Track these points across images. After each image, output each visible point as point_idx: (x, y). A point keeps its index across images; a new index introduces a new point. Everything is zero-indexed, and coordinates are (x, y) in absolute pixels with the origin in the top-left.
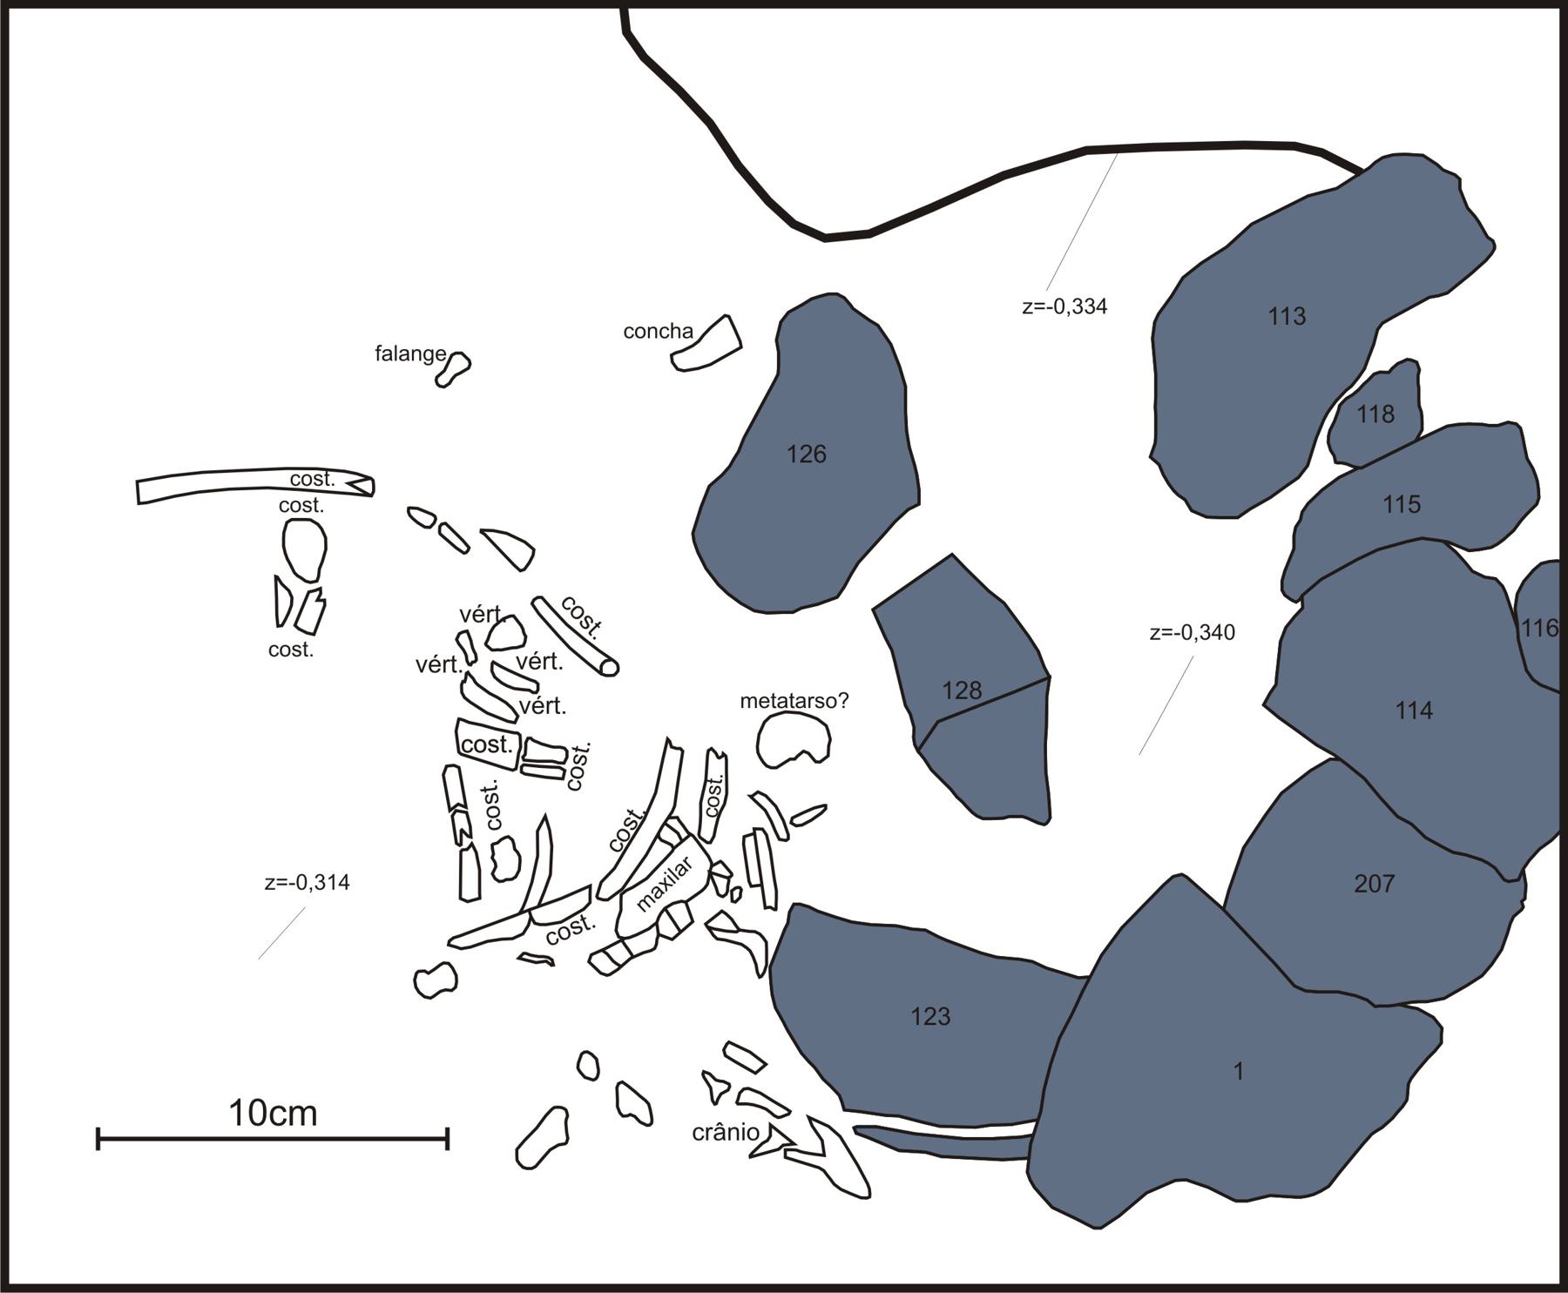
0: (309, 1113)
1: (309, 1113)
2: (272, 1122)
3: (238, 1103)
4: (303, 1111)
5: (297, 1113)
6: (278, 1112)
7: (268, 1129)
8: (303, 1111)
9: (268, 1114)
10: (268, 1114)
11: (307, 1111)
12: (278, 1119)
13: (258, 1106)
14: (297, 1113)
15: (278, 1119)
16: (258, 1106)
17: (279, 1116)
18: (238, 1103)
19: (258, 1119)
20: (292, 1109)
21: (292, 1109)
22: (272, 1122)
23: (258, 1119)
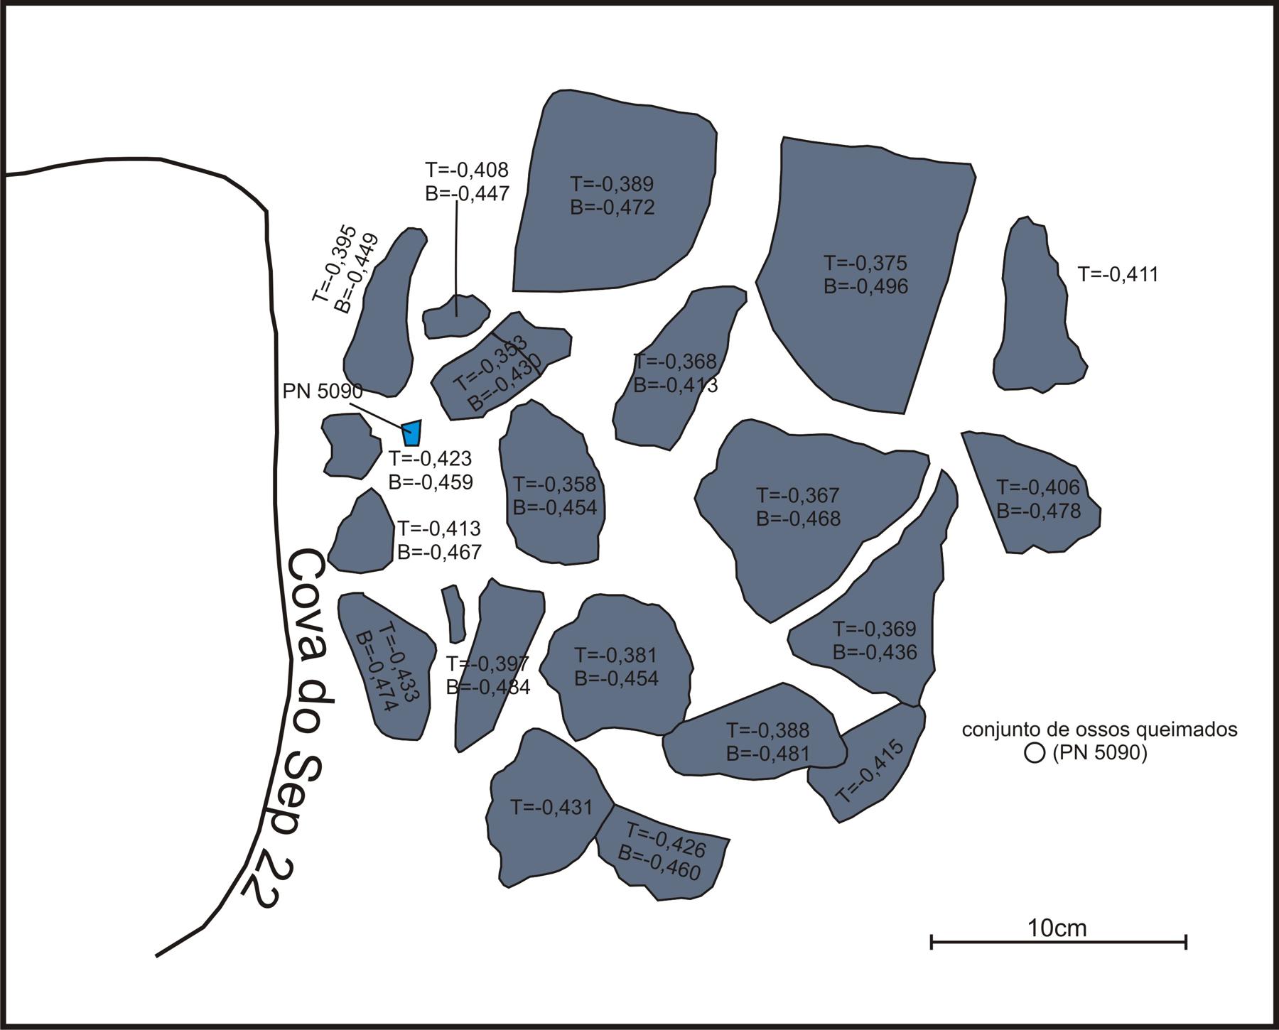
0: (1081, 928)
1: (1081, 928)
2: (1053, 933)
3: (1034, 921)
5: (1073, 928)
7: (1054, 937)
12: (1061, 932)
13: (1047, 923)
14: (1073, 928)
15: (1061, 932)
16: (1047, 923)
17: (1061, 930)
18: (1034, 921)
19: (1047, 931)
22: (1053, 933)
23: (1047, 931)
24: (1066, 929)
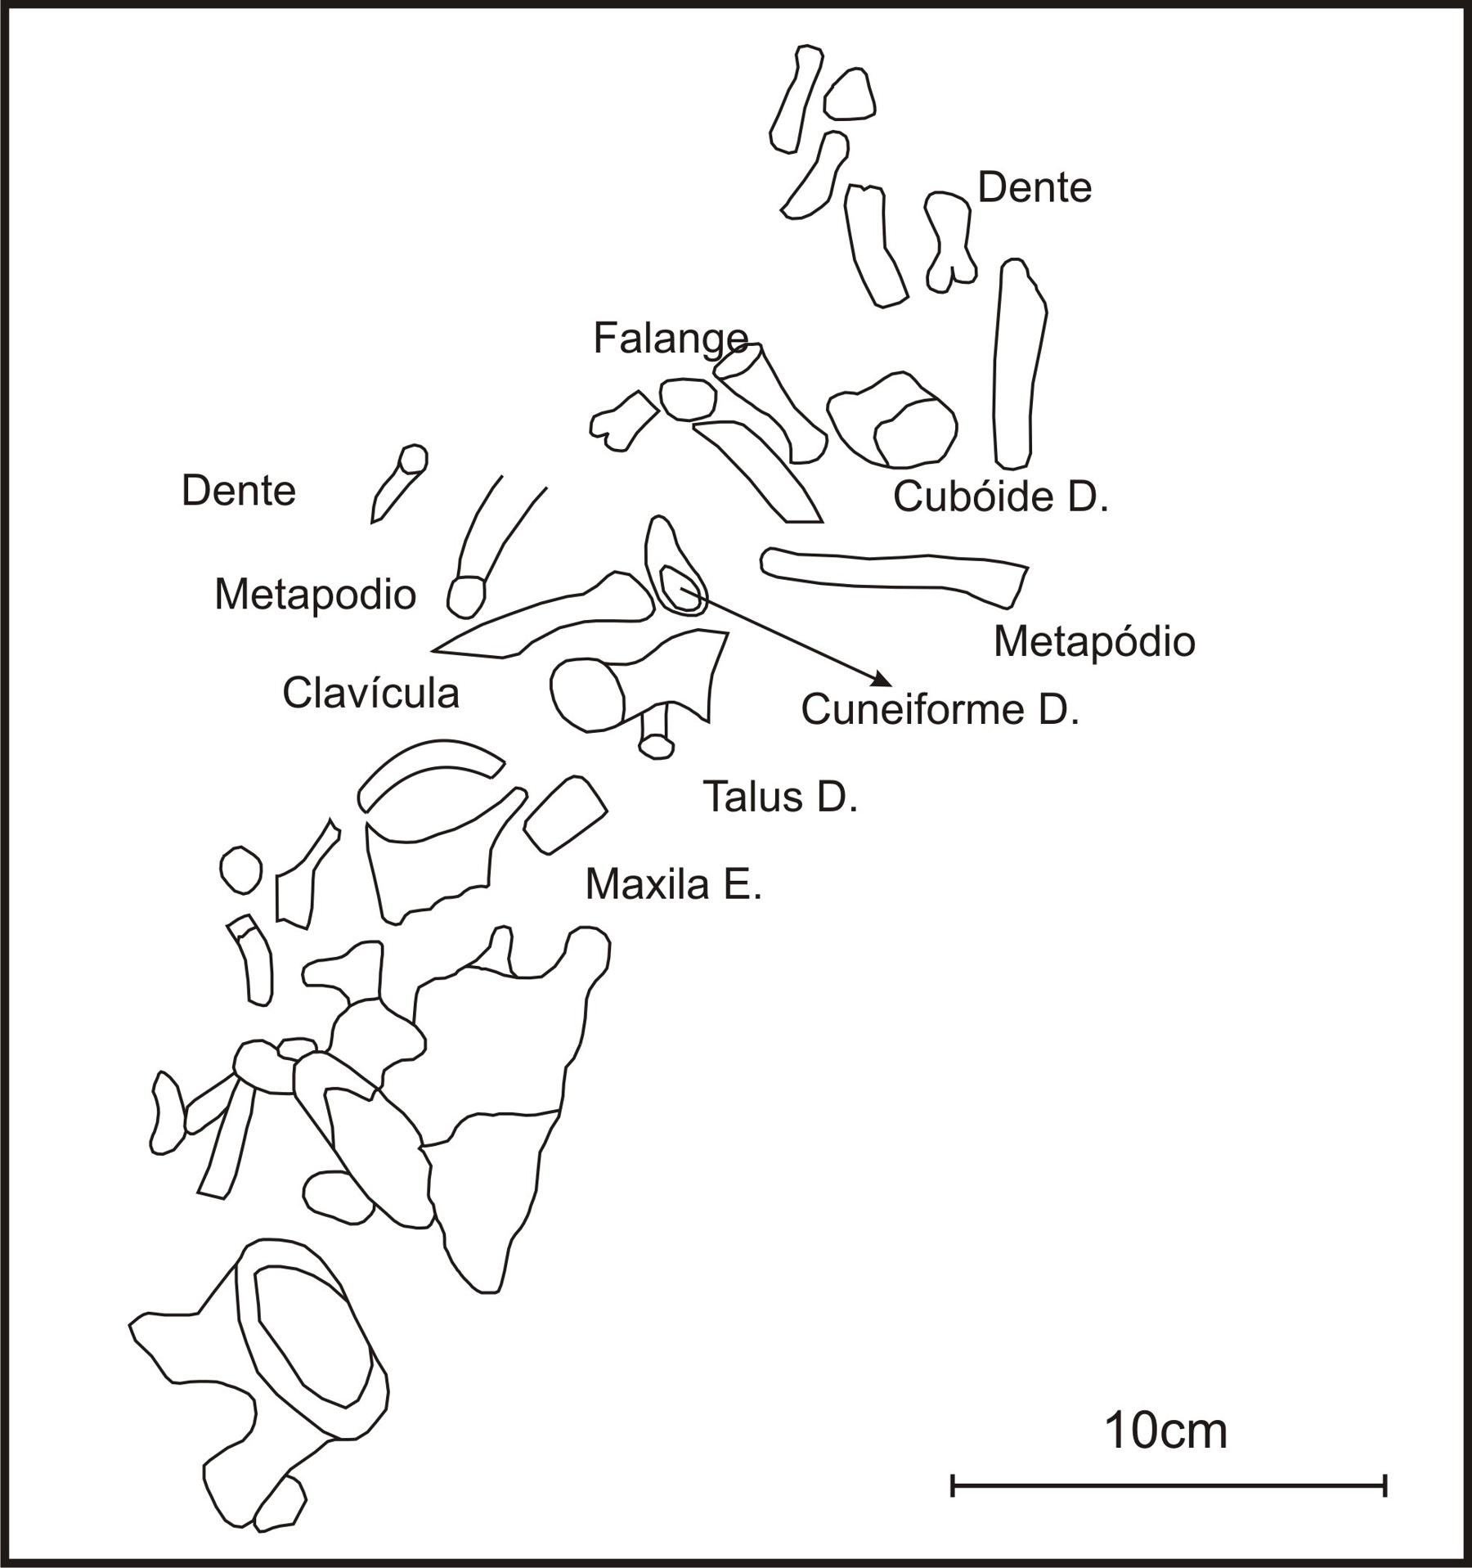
0: (1216, 1431)
1: (1216, 1431)
4: (1208, 1427)
5: (1200, 1430)
6: (1173, 1428)
9: (1160, 1433)
10: (1160, 1433)
11: (1212, 1430)
12: (1173, 1440)
13: (1145, 1423)
14: (1200, 1430)
15: (1173, 1440)
16: (1145, 1423)
17: (1174, 1435)
19: (1145, 1438)
20: (1192, 1425)
21: (1192, 1425)
23: (1145, 1435)
24: (1185, 1433)
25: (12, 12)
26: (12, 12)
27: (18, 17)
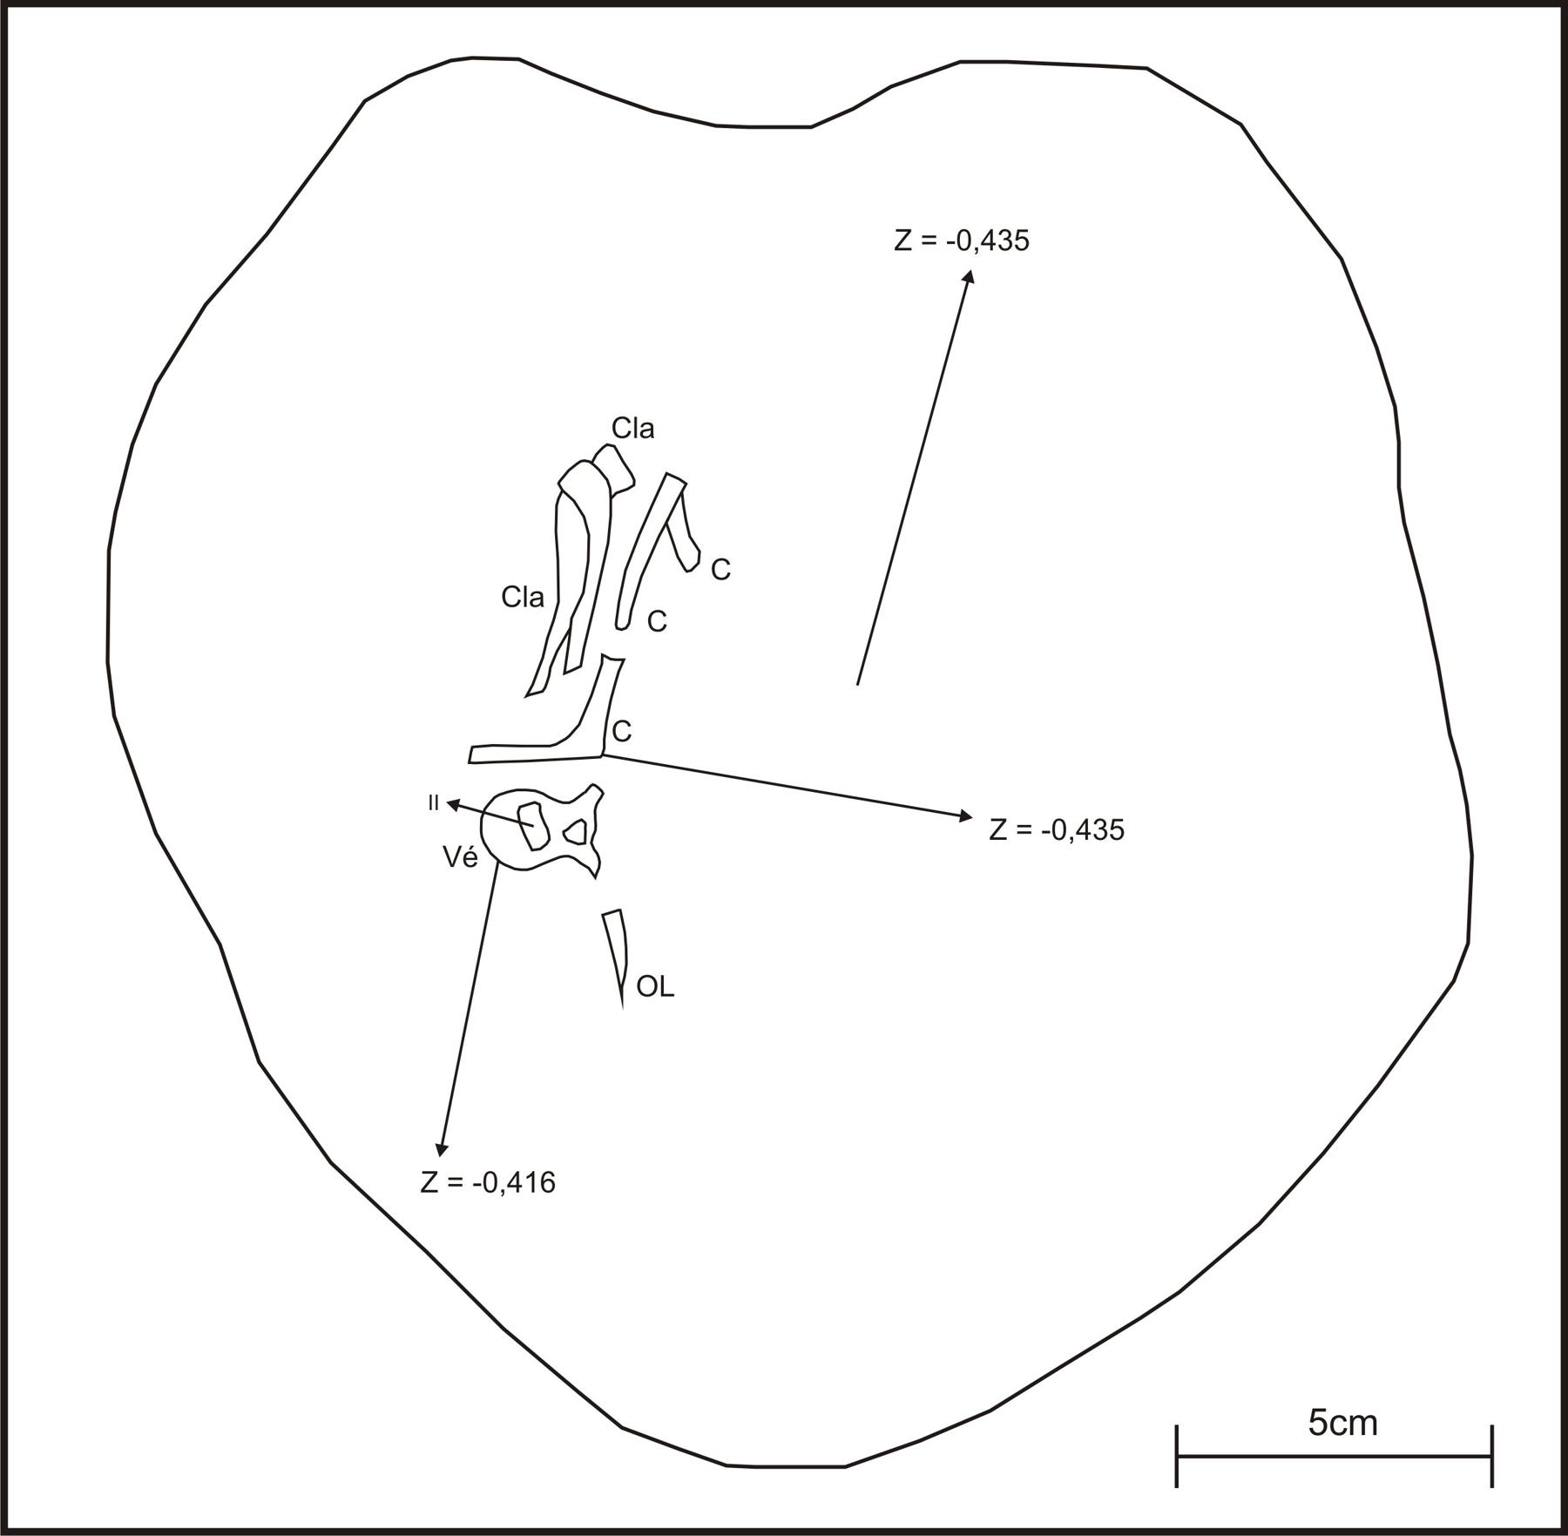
0: (1369, 1422)
1: (1369, 1422)
4: (1363, 1420)
5: (1358, 1422)
6: (1338, 1422)
8: (1363, 1420)
10: (1329, 1426)
11: (1366, 1422)
12: (1338, 1429)
14: (1358, 1422)
15: (1338, 1429)
20: (1352, 1419)
21: (1352, 1419)
24: (1347, 1425)
25: (11, 10)
26: (11, 10)
27: (14, 13)
